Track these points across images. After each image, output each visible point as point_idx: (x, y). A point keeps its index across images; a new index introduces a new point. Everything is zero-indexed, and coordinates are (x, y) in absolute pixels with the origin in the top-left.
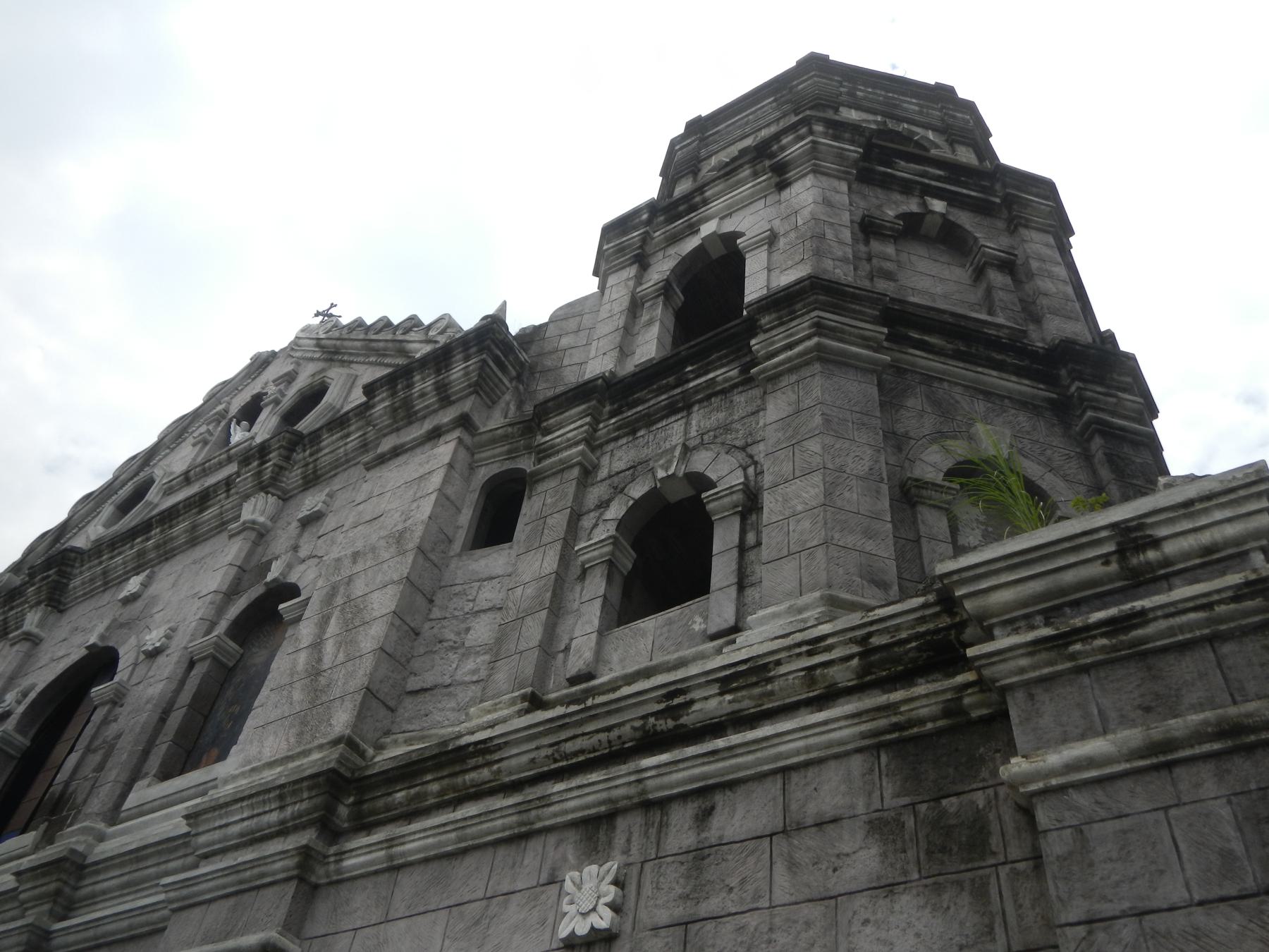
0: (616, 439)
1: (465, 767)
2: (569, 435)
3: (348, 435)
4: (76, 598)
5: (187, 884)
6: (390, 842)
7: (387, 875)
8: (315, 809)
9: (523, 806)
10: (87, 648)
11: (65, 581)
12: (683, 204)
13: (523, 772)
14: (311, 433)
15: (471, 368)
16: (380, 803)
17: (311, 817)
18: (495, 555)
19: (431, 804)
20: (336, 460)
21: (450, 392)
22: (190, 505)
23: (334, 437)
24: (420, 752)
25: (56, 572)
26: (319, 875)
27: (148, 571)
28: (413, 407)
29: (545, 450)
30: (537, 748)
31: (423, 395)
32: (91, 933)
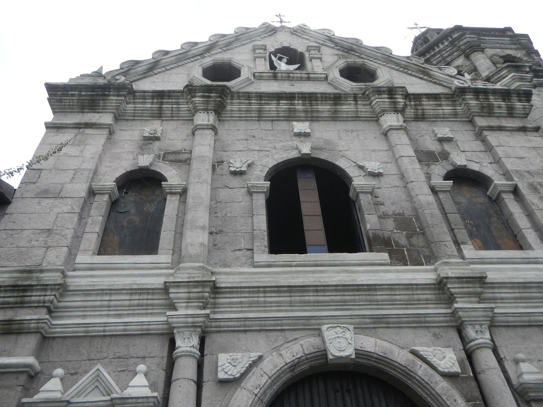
4: (232, 117)
12: (541, 72)
20: (437, 115)
23: (431, 103)
28: (493, 110)
32: (526, 319)
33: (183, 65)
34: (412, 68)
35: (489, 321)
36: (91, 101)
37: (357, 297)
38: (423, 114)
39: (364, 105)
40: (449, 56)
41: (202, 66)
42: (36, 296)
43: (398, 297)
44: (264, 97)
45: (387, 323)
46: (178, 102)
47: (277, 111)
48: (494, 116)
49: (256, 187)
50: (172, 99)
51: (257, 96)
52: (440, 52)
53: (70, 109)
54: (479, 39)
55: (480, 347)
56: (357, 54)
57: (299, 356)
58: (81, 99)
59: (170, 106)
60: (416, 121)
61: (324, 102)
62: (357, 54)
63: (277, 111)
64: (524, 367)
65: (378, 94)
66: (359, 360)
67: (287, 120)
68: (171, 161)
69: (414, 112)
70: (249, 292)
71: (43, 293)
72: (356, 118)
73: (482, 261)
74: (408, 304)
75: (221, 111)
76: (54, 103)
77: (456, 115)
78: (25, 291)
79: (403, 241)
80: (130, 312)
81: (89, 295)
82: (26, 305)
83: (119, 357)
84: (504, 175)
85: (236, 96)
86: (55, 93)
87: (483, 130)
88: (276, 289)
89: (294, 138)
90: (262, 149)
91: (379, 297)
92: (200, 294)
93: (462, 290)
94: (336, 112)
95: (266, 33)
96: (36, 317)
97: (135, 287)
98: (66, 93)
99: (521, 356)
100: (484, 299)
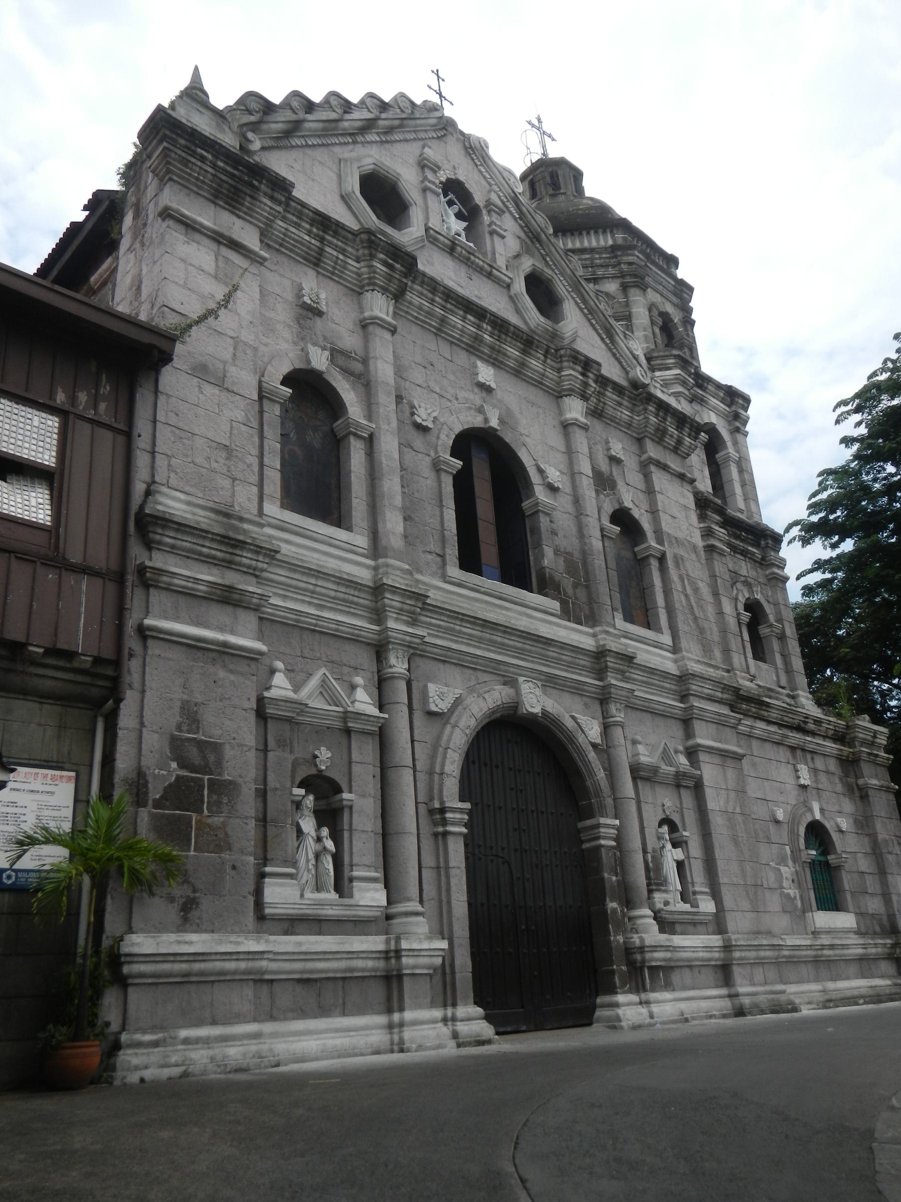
4: (407, 313)
6: (752, 727)
16: (739, 705)
32: (647, 704)
33: (328, 145)
34: (599, 317)
36: (233, 190)
37: (534, 649)
38: (602, 411)
39: (552, 368)
40: (602, 266)
41: (362, 169)
42: (246, 557)
43: (564, 657)
44: (452, 298)
45: (556, 684)
46: (345, 250)
47: (462, 331)
48: (662, 445)
49: (448, 464)
50: (338, 240)
51: (443, 293)
52: (592, 250)
53: (197, 186)
54: (646, 265)
55: (616, 724)
56: (542, 251)
57: (499, 703)
58: (218, 178)
59: (335, 253)
61: (514, 342)
62: (542, 251)
63: (462, 331)
64: (641, 748)
67: (467, 351)
68: (341, 369)
70: (448, 616)
71: (255, 557)
72: (538, 384)
73: (626, 635)
74: (570, 666)
76: (174, 159)
77: (630, 425)
78: (234, 546)
79: (570, 591)
80: (334, 606)
81: (295, 571)
82: (234, 567)
83: (332, 662)
84: (655, 532)
85: (420, 279)
86: (174, 136)
87: (650, 462)
89: (476, 390)
90: (444, 394)
91: (551, 654)
92: (413, 608)
94: (523, 364)
95: (434, 130)
96: (259, 591)
97: (345, 577)
98: (193, 148)
99: (639, 738)
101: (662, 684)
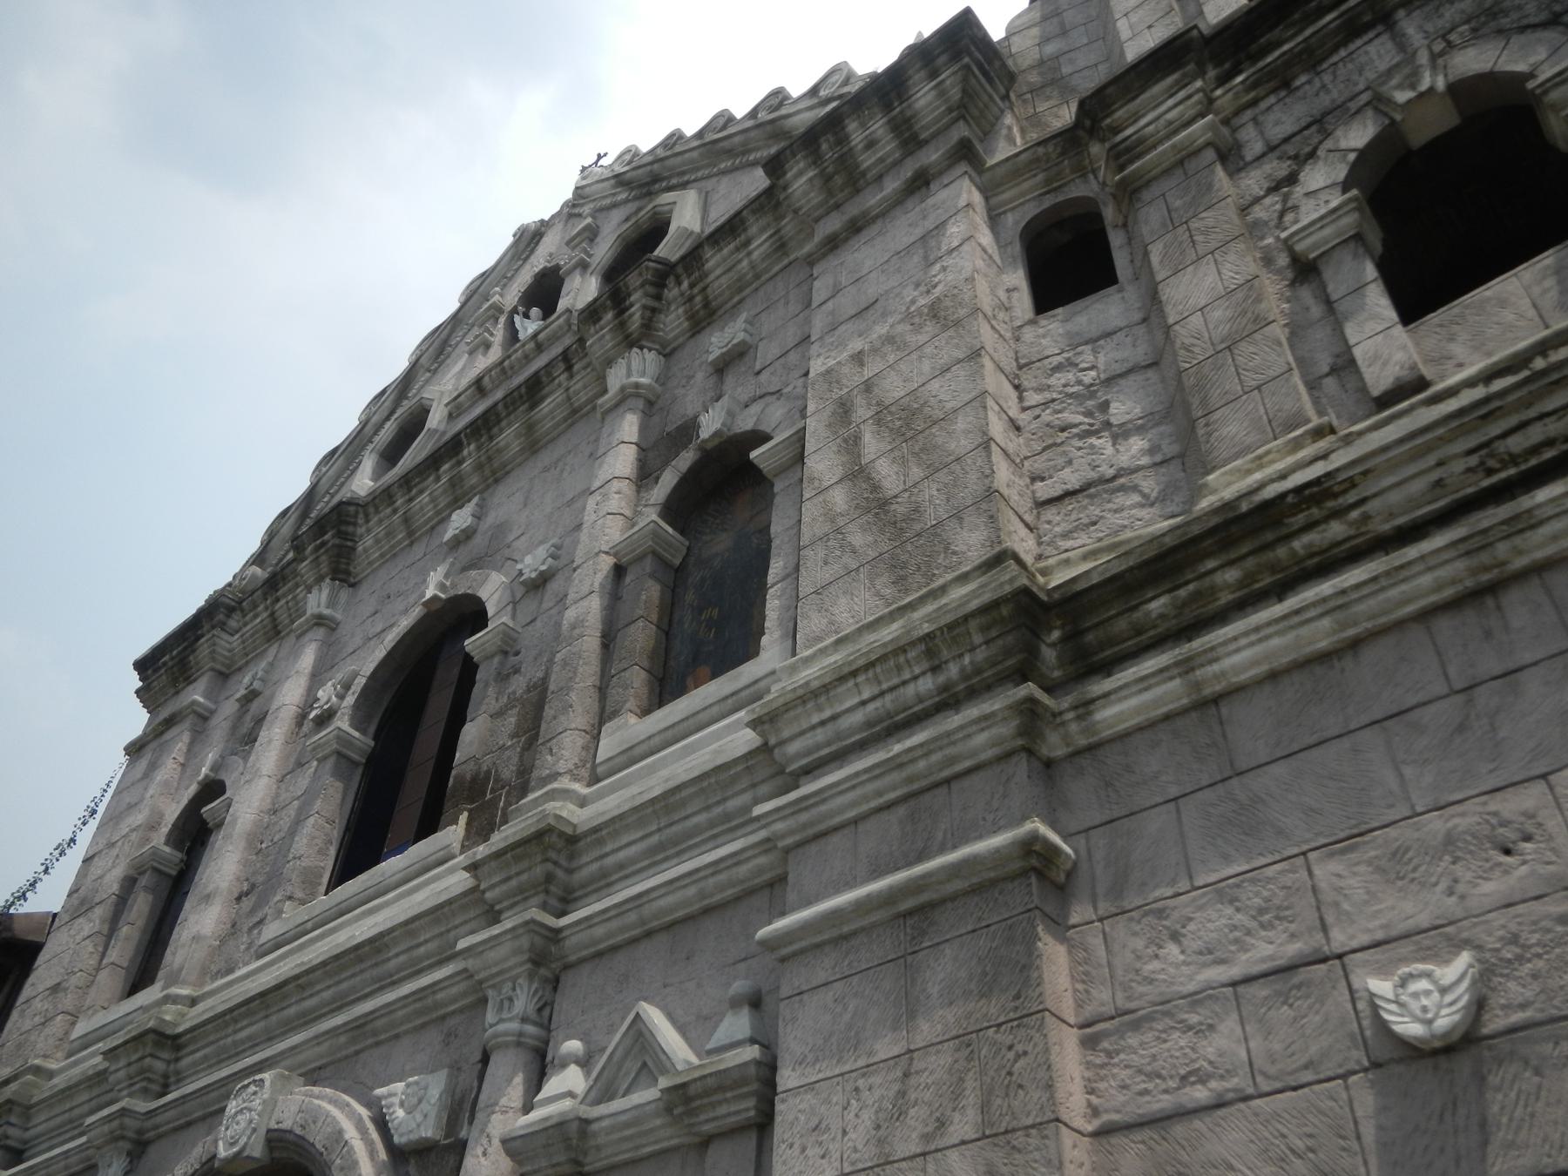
0: (1254, 103)
1: (1285, 531)
2: (1169, 116)
3: (748, 242)
5: (804, 804)
7: (1194, 715)
8: (1008, 653)
9: (1471, 541)
10: (426, 604)
11: (349, 544)
13: (1419, 507)
14: (683, 258)
15: (948, 82)
16: (1122, 625)
17: (1000, 667)
18: (1098, 306)
19: (1228, 603)
20: (739, 280)
21: (916, 127)
22: (513, 403)
23: (725, 251)
24: (1179, 532)
25: (333, 537)
26: (1054, 745)
27: (476, 500)
28: (858, 167)
29: (1128, 150)
30: (1440, 464)
31: (871, 144)
32: (632, 917)
35: (532, 961)
45: (375, 1033)
48: (869, 184)
60: (699, 332)
65: (595, 323)
66: (277, 1154)
69: (686, 312)
75: (348, 564)
88: (243, 1009)
93: (504, 887)
100: (583, 886)
101: (718, 810)
